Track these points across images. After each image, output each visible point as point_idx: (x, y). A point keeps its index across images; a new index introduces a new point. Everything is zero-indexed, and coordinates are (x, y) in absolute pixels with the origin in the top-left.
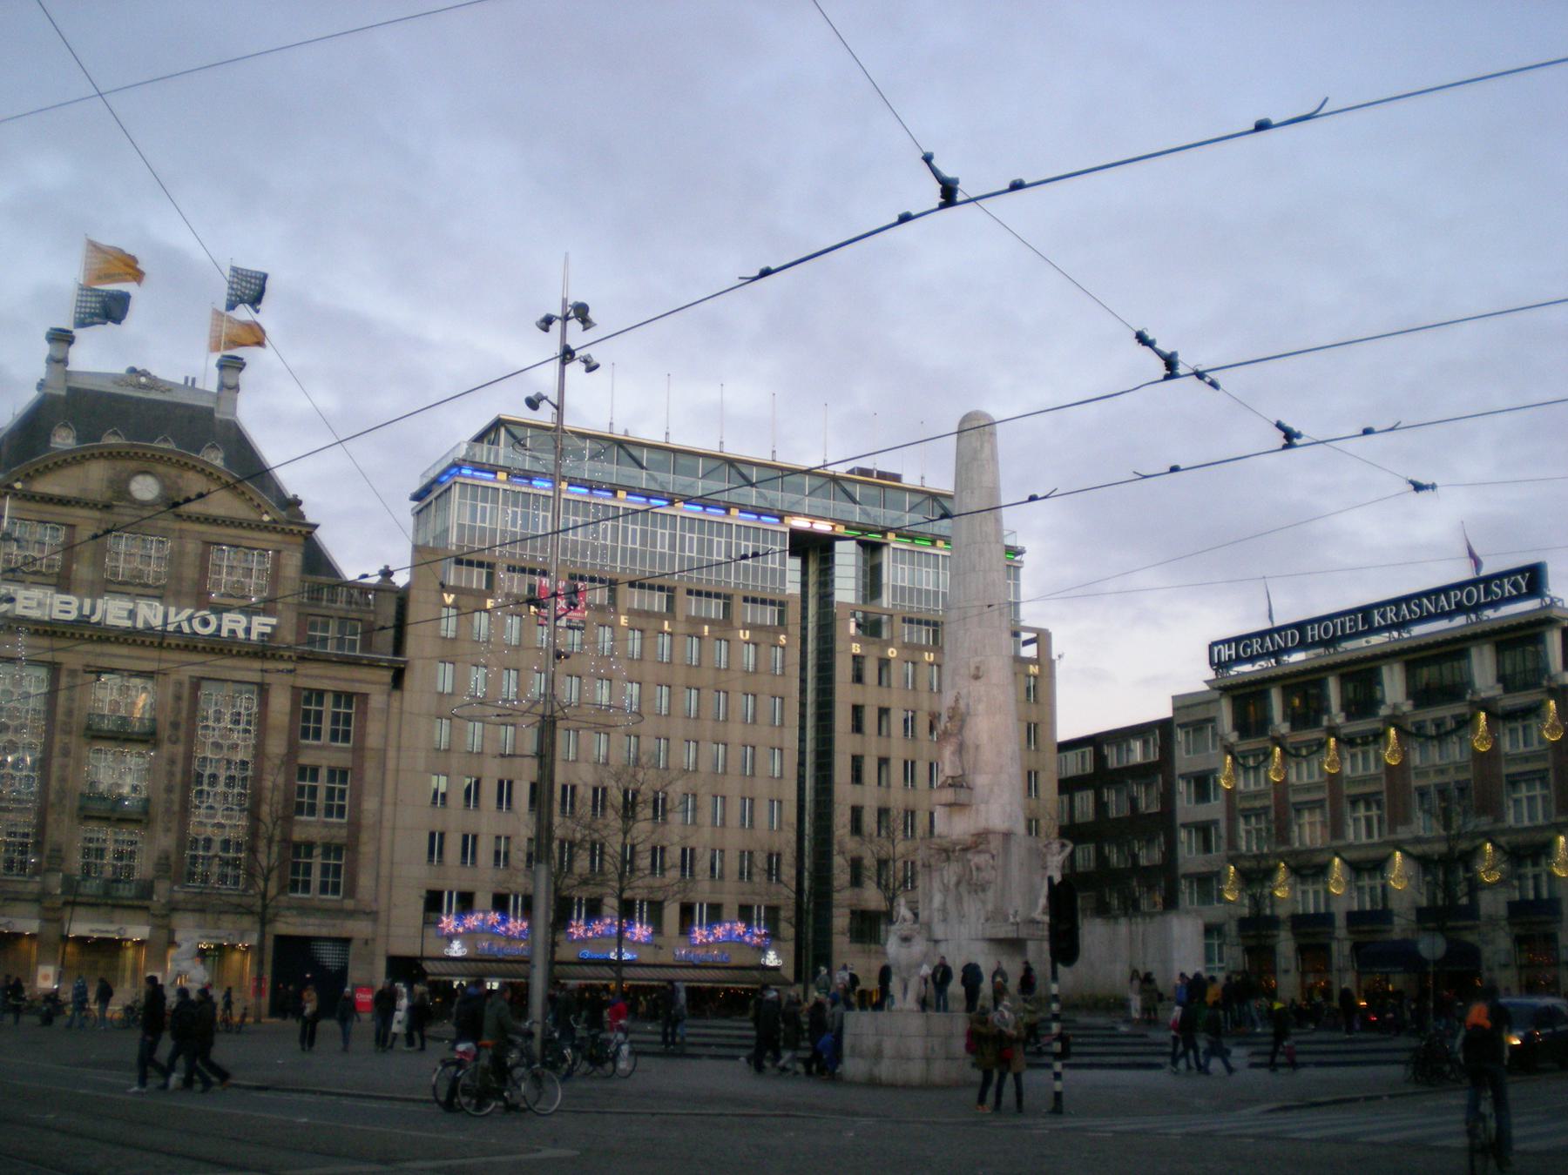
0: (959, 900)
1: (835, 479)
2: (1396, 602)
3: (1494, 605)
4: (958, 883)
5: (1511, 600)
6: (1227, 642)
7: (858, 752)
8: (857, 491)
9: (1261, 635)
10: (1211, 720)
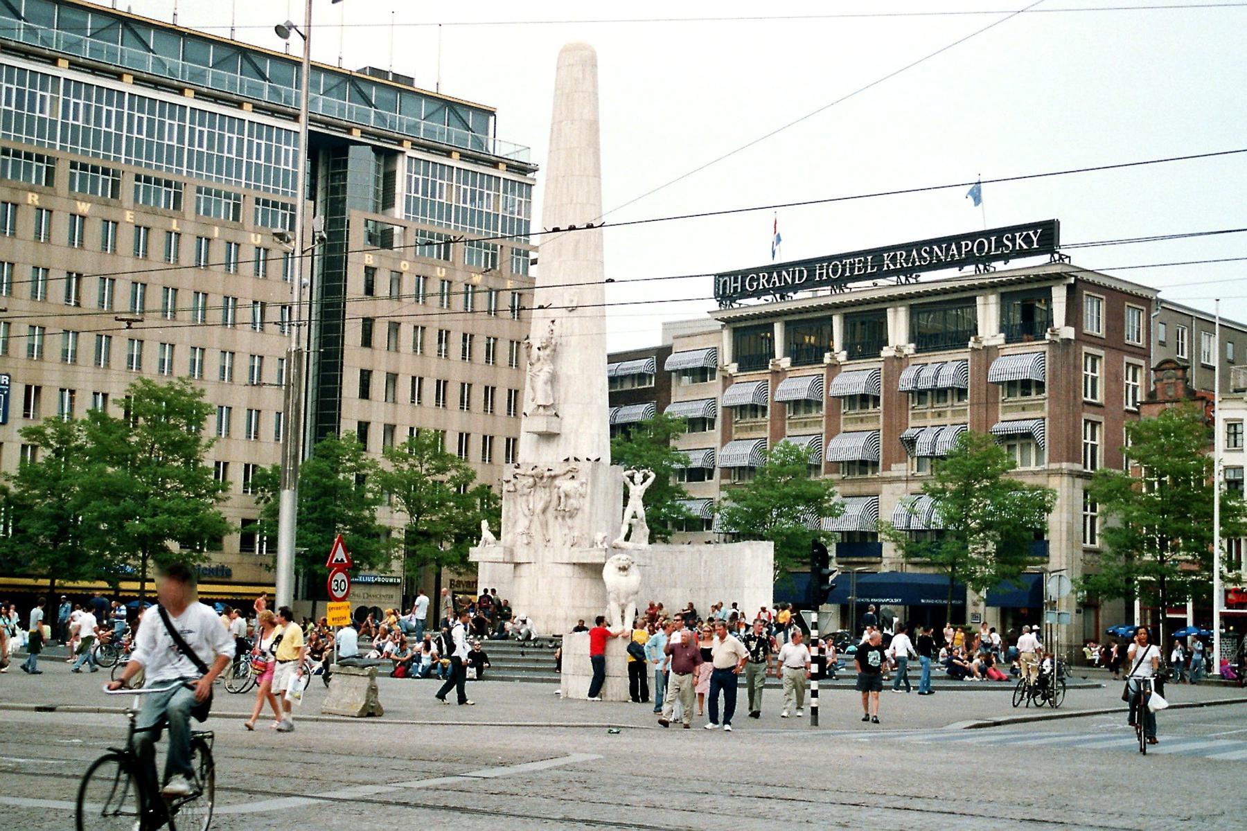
0: (545, 525)
1: (349, 78)
2: (908, 247)
3: (1006, 258)
4: (544, 511)
5: (1022, 254)
6: (734, 274)
7: (368, 367)
8: (374, 93)
9: (770, 269)
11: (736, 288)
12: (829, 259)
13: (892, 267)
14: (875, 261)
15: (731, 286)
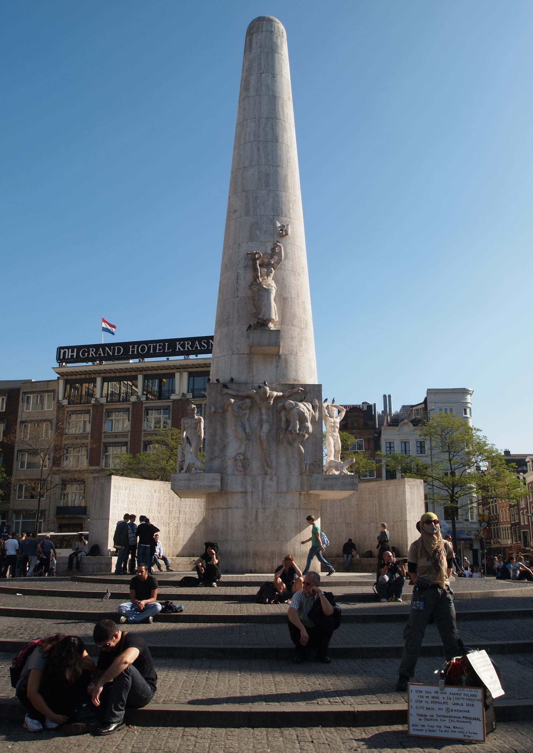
2: (193, 340)
6: (72, 348)
10: (53, 391)
11: (72, 356)
12: (139, 343)
13: (182, 349)
14: (170, 346)
15: (64, 355)
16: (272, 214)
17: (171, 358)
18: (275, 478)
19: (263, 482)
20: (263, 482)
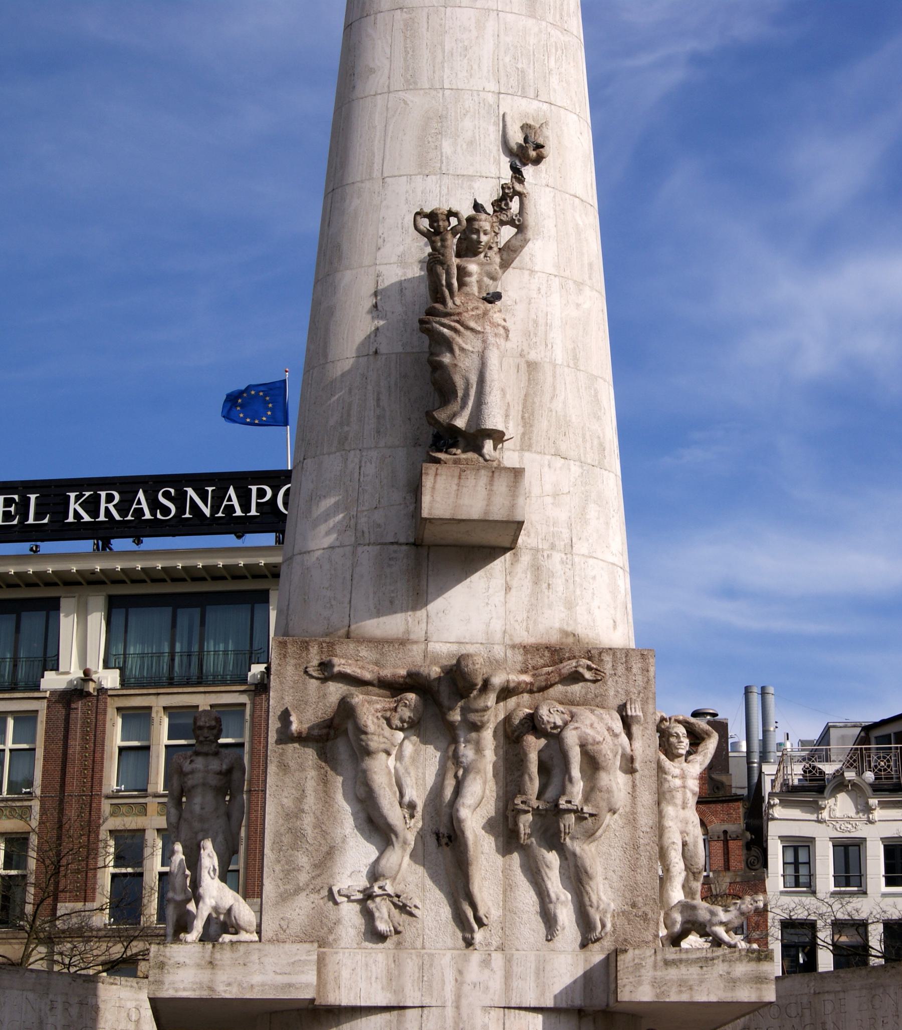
2: (127, 486)
13: (87, 518)
16: (492, 86)
17: (47, 547)
18: (497, 959)
19: (460, 972)
20: (460, 972)
